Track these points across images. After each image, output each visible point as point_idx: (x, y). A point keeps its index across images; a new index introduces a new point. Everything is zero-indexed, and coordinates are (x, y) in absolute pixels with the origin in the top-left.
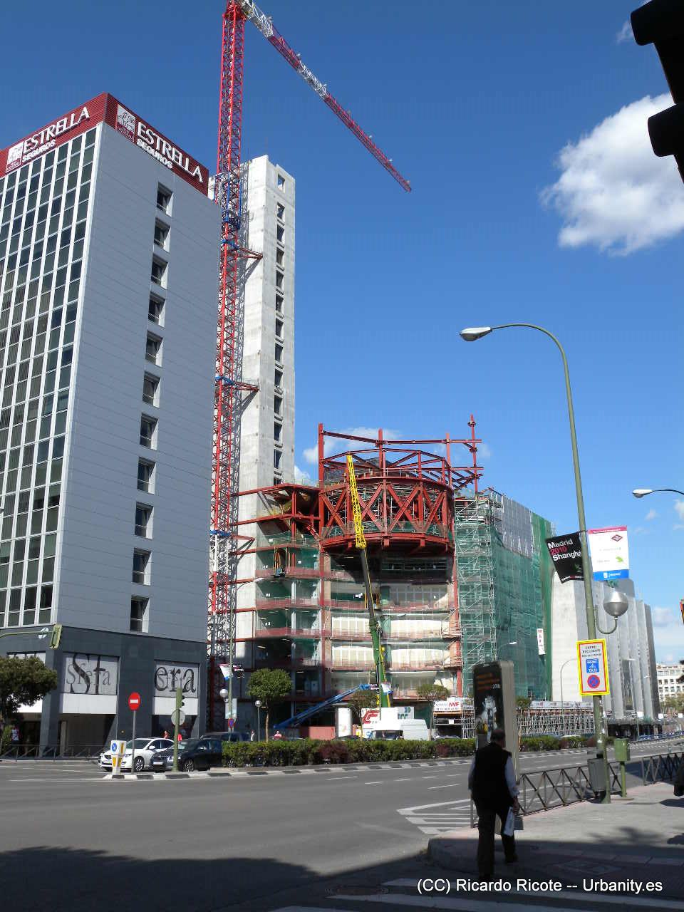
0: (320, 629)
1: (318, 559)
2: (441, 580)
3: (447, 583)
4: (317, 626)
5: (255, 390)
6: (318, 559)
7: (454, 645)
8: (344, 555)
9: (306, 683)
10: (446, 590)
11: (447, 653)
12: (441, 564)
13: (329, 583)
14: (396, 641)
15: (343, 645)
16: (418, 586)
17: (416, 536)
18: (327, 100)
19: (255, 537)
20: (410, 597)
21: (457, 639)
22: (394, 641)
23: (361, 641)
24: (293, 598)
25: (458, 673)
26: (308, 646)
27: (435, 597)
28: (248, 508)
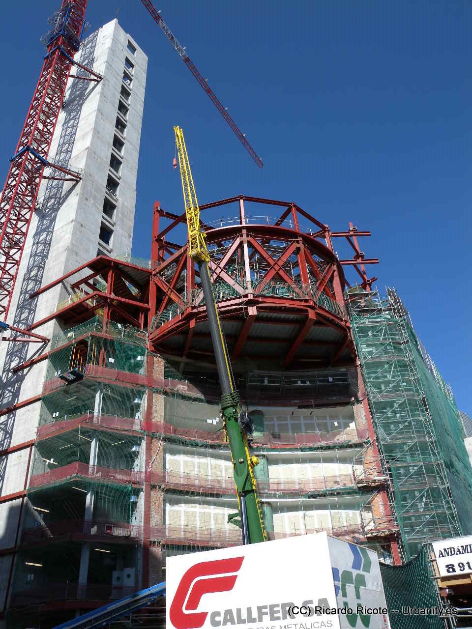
0: (144, 470)
1: (145, 364)
2: (343, 399)
3: (353, 404)
4: (140, 465)
5: (77, 179)
6: (145, 364)
7: (379, 501)
8: (187, 352)
9: (115, 574)
10: (351, 417)
11: (368, 516)
12: (343, 377)
13: (161, 398)
14: (280, 497)
15: (186, 502)
16: (309, 411)
17: (303, 304)
18: (187, 60)
19: (50, 337)
20: (297, 428)
21: (382, 488)
22: (275, 496)
23: (219, 496)
24: (96, 414)
25: (394, 546)
26: (122, 500)
27: (336, 424)
28: (49, 304)
